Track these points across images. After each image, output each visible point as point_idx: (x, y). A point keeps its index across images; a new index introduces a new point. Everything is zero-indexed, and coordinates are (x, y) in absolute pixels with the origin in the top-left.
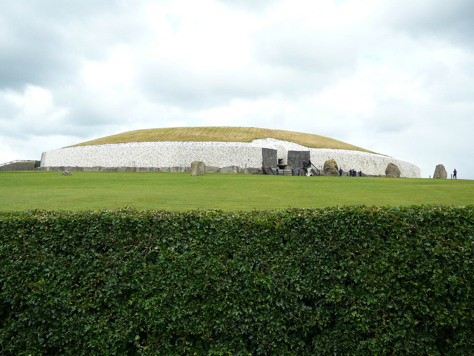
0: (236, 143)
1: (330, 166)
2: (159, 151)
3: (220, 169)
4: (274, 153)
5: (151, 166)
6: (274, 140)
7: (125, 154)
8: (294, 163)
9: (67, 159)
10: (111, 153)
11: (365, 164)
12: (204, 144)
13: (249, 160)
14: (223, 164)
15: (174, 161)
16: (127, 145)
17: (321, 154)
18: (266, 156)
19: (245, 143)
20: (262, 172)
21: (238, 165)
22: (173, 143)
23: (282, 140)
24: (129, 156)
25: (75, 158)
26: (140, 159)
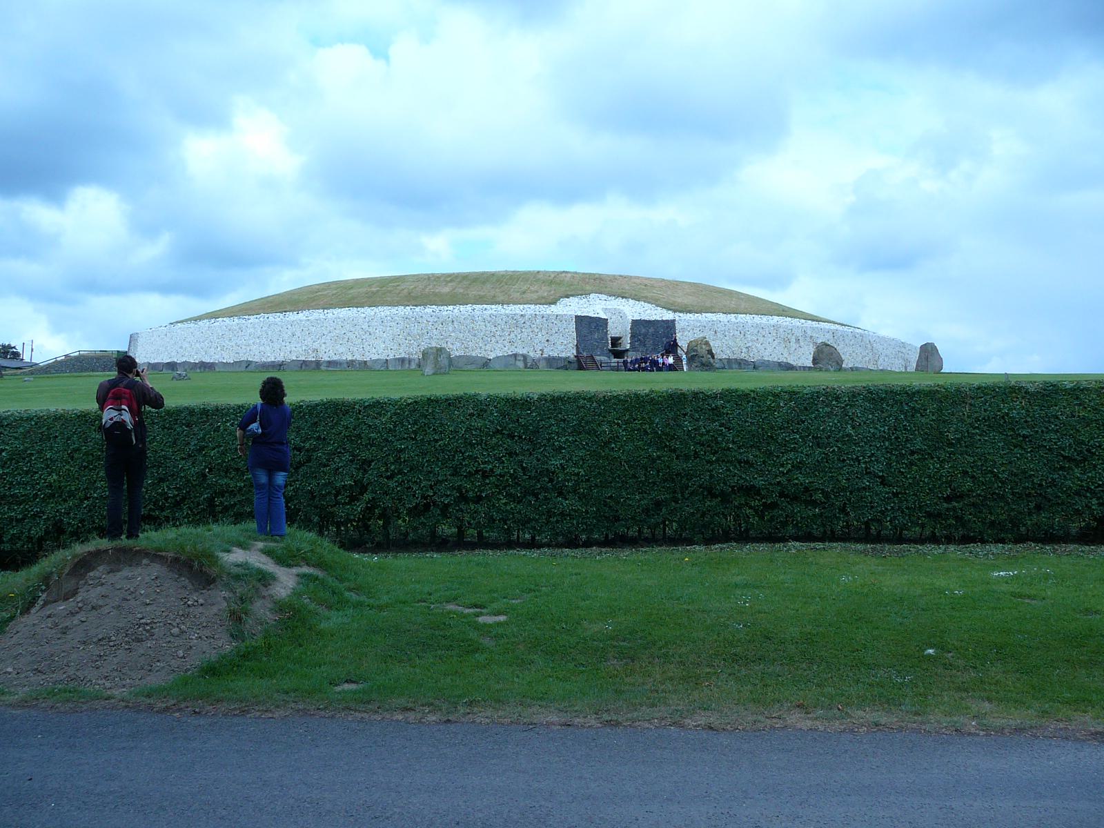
0: (521, 307)
1: (696, 351)
2: (365, 326)
3: (490, 360)
4: (601, 326)
5: (350, 358)
6: (604, 297)
7: (298, 334)
8: (645, 345)
9: (181, 347)
10: (270, 333)
11: (793, 345)
12: (456, 311)
13: (548, 341)
14: (495, 351)
15: (396, 347)
16: (302, 316)
17: (699, 324)
18: (585, 331)
19: (541, 306)
20: (576, 365)
21: (525, 352)
22: (394, 310)
23: (623, 298)
24: (306, 338)
25: (198, 345)
26: (328, 345)
